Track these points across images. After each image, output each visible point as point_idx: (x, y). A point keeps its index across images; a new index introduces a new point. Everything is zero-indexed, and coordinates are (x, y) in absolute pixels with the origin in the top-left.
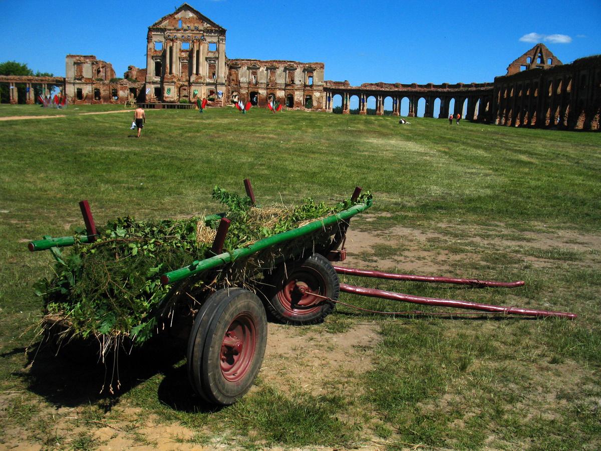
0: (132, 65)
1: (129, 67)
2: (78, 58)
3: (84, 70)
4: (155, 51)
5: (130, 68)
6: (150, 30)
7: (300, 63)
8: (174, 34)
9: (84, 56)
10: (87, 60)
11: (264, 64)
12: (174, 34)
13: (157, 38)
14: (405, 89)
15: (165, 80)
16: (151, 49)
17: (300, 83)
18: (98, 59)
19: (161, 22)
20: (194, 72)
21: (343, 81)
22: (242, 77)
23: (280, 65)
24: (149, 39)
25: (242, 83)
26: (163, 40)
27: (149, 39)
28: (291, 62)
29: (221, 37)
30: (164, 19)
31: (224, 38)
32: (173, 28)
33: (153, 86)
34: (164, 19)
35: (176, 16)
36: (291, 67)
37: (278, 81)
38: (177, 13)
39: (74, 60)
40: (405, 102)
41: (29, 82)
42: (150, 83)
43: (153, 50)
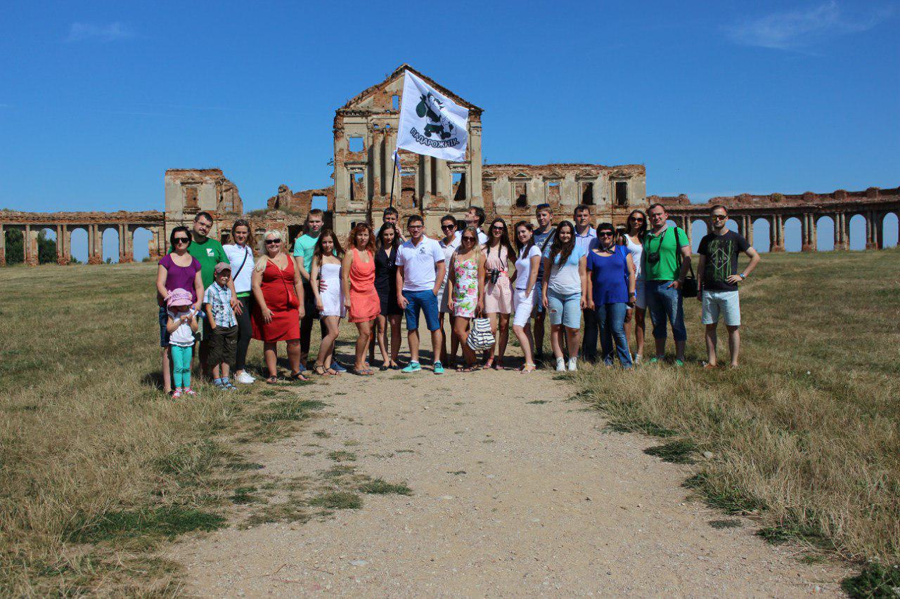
0: (287, 184)
1: (280, 188)
2: (188, 174)
3: (200, 195)
4: (351, 153)
5: (283, 189)
6: (339, 114)
7: (602, 168)
8: (386, 121)
9: (201, 171)
10: (207, 178)
11: (536, 172)
12: (386, 121)
13: (355, 128)
14: (792, 204)
15: (374, 207)
16: (341, 150)
17: (604, 203)
18: (226, 175)
19: (360, 98)
20: (429, 188)
21: (676, 195)
22: (499, 196)
23: (566, 172)
24: (337, 131)
25: (500, 207)
26: (364, 131)
27: (337, 131)
28: (588, 165)
29: (473, 124)
30: (367, 93)
31: (478, 125)
32: (383, 110)
33: (350, 219)
34: (367, 93)
35: (387, 89)
36: (588, 174)
37: (564, 202)
38: (386, 83)
39: (182, 177)
40: (859, 223)
41: (93, 222)
42: (341, 213)
43: (346, 152)
